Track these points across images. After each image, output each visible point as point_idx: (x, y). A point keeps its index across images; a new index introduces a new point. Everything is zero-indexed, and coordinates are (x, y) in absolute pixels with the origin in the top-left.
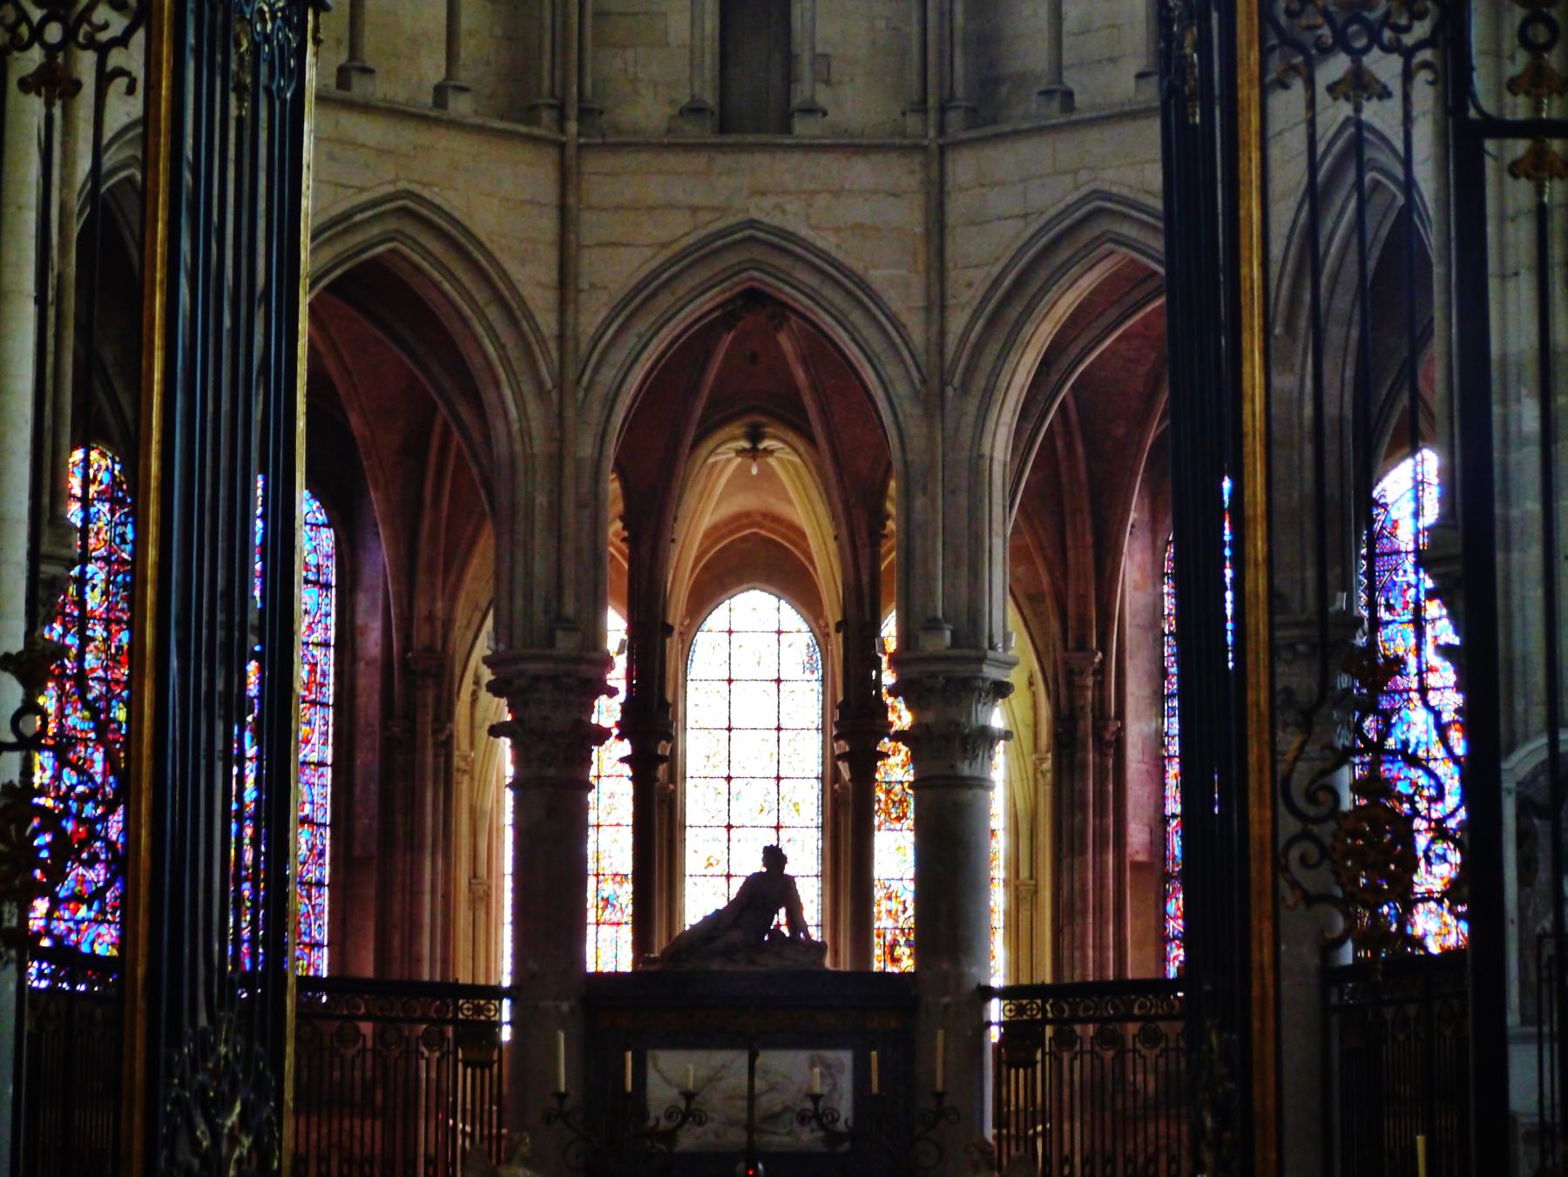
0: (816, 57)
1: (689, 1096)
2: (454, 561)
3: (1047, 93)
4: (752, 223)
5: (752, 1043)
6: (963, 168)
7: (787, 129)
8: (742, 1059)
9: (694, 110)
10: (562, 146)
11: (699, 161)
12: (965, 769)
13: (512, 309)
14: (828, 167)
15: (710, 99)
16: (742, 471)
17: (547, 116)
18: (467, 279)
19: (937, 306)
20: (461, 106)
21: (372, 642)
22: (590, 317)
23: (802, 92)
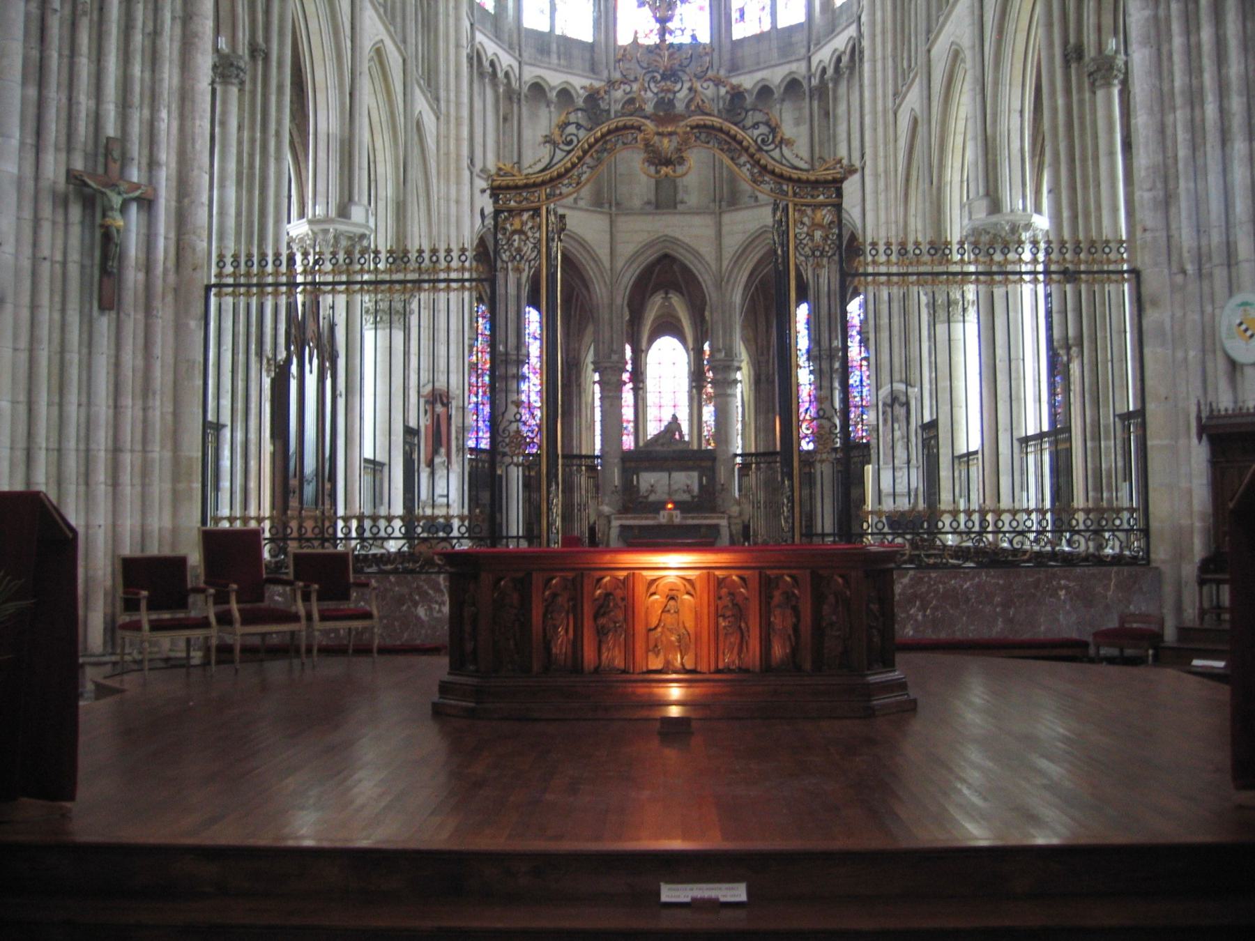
0: (683, 186)
1: (652, 486)
2: (581, 332)
3: (751, 197)
4: (666, 236)
5: (670, 470)
6: (726, 218)
7: (675, 207)
8: (665, 475)
9: (649, 203)
10: (611, 214)
11: (650, 218)
12: (729, 391)
13: (596, 260)
14: (688, 218)
15: (653, 199)
16: (662, 304)
17: (607, 206)
18: (585, 255)
19: (719, 258)
20: (581, 204)
22: (620, 264)
23: (679, 197)
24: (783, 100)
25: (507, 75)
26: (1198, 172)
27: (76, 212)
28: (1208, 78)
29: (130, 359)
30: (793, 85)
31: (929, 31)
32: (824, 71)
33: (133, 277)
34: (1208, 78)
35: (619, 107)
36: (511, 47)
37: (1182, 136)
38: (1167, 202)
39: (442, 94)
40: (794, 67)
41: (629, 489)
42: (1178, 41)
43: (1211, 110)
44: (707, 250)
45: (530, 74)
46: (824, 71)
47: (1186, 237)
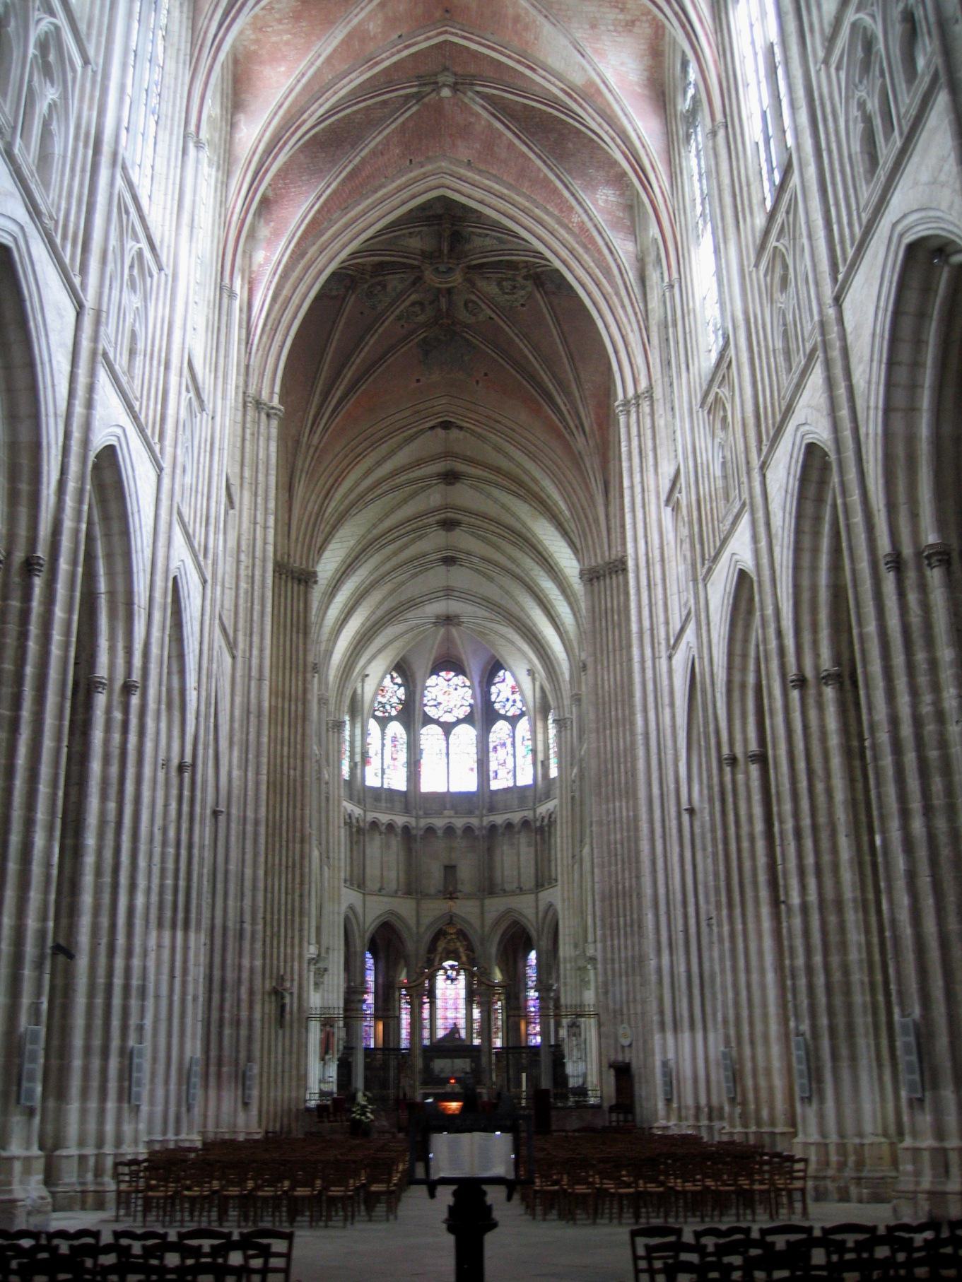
6: (487, 902)
9: (440, 892)
19: (483, 926)
20: (400, 893)
21: (380, 980)
24: (519, 832)
25: (358, 821)
26: (614, 985)
27: (273, 998)
28: (616, 956)
29: (287, 1043)
30: (525, 823)
31: (581, 841)
32: (543, 818)
33: (288, 1017)
34: (616, 956)
35: (421, 832)
36: (359, 802)
37: (610, 973)
38: (606, 993)
39: (331, 855)
40: (526, 813)
41: (427, 1069)
42: (609, 943)
43: (617, 966)
44: (476, 922)
45: (371, 816)
46: (543, 818)
47: (611, 1006)
